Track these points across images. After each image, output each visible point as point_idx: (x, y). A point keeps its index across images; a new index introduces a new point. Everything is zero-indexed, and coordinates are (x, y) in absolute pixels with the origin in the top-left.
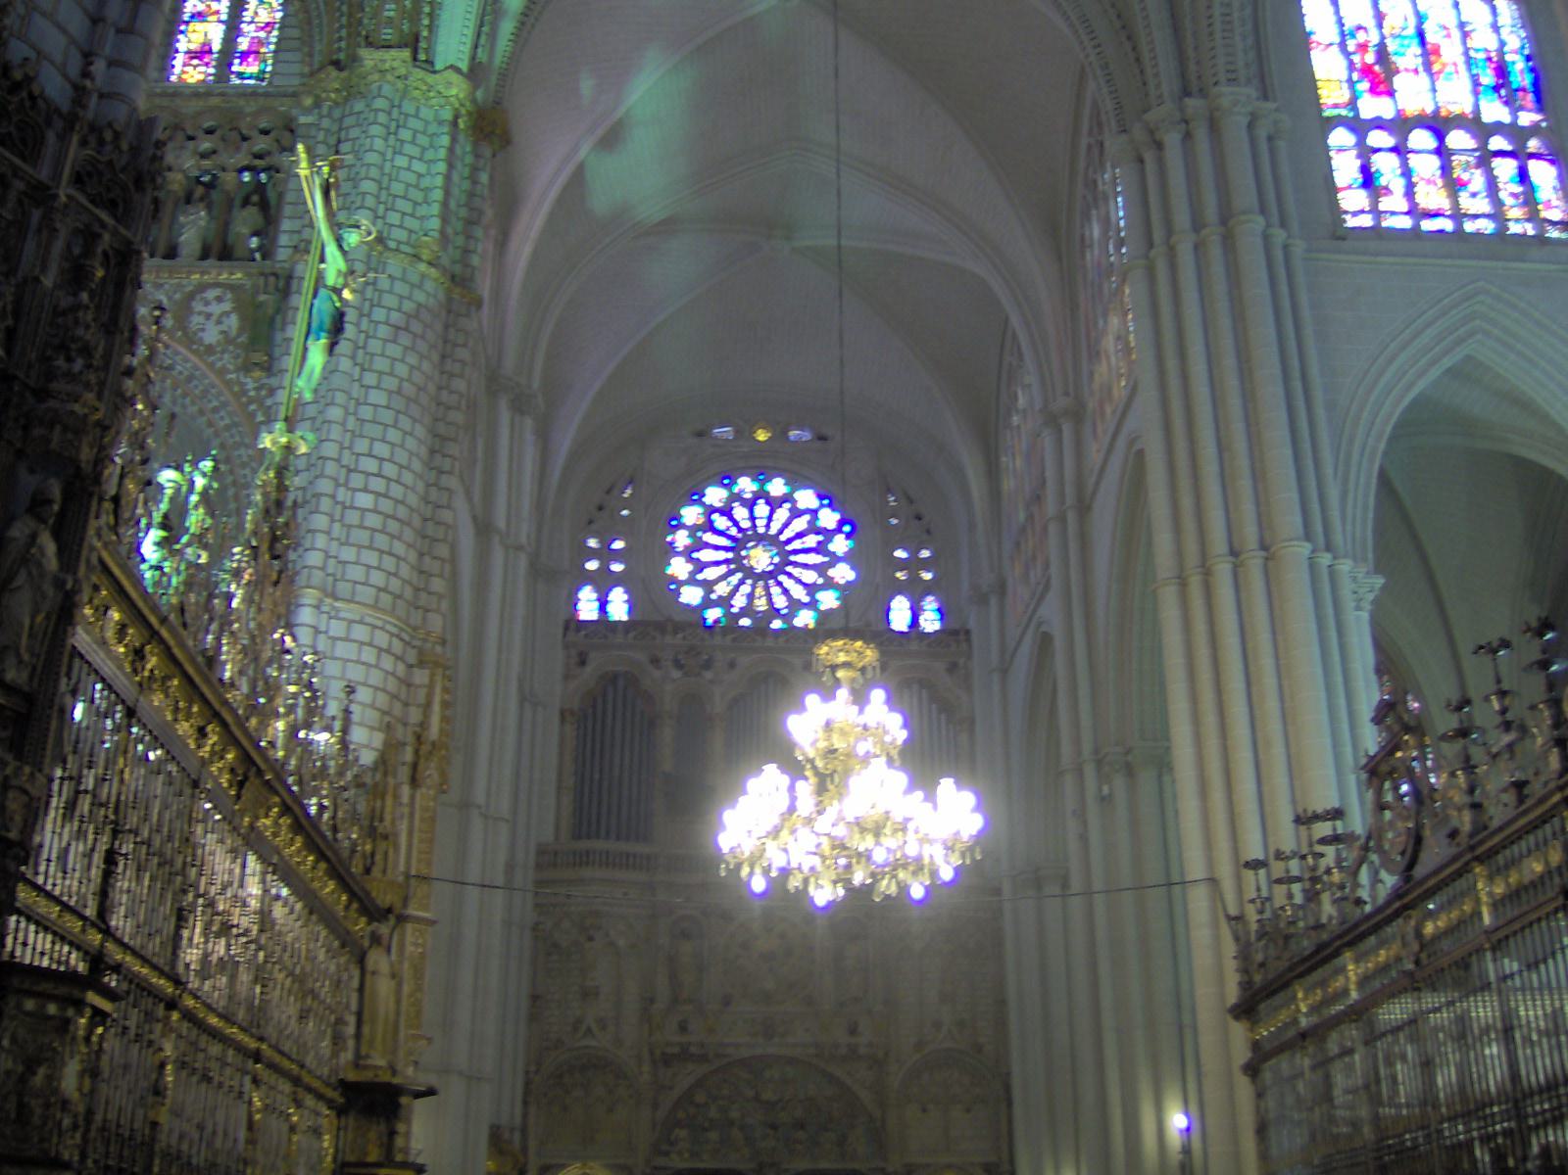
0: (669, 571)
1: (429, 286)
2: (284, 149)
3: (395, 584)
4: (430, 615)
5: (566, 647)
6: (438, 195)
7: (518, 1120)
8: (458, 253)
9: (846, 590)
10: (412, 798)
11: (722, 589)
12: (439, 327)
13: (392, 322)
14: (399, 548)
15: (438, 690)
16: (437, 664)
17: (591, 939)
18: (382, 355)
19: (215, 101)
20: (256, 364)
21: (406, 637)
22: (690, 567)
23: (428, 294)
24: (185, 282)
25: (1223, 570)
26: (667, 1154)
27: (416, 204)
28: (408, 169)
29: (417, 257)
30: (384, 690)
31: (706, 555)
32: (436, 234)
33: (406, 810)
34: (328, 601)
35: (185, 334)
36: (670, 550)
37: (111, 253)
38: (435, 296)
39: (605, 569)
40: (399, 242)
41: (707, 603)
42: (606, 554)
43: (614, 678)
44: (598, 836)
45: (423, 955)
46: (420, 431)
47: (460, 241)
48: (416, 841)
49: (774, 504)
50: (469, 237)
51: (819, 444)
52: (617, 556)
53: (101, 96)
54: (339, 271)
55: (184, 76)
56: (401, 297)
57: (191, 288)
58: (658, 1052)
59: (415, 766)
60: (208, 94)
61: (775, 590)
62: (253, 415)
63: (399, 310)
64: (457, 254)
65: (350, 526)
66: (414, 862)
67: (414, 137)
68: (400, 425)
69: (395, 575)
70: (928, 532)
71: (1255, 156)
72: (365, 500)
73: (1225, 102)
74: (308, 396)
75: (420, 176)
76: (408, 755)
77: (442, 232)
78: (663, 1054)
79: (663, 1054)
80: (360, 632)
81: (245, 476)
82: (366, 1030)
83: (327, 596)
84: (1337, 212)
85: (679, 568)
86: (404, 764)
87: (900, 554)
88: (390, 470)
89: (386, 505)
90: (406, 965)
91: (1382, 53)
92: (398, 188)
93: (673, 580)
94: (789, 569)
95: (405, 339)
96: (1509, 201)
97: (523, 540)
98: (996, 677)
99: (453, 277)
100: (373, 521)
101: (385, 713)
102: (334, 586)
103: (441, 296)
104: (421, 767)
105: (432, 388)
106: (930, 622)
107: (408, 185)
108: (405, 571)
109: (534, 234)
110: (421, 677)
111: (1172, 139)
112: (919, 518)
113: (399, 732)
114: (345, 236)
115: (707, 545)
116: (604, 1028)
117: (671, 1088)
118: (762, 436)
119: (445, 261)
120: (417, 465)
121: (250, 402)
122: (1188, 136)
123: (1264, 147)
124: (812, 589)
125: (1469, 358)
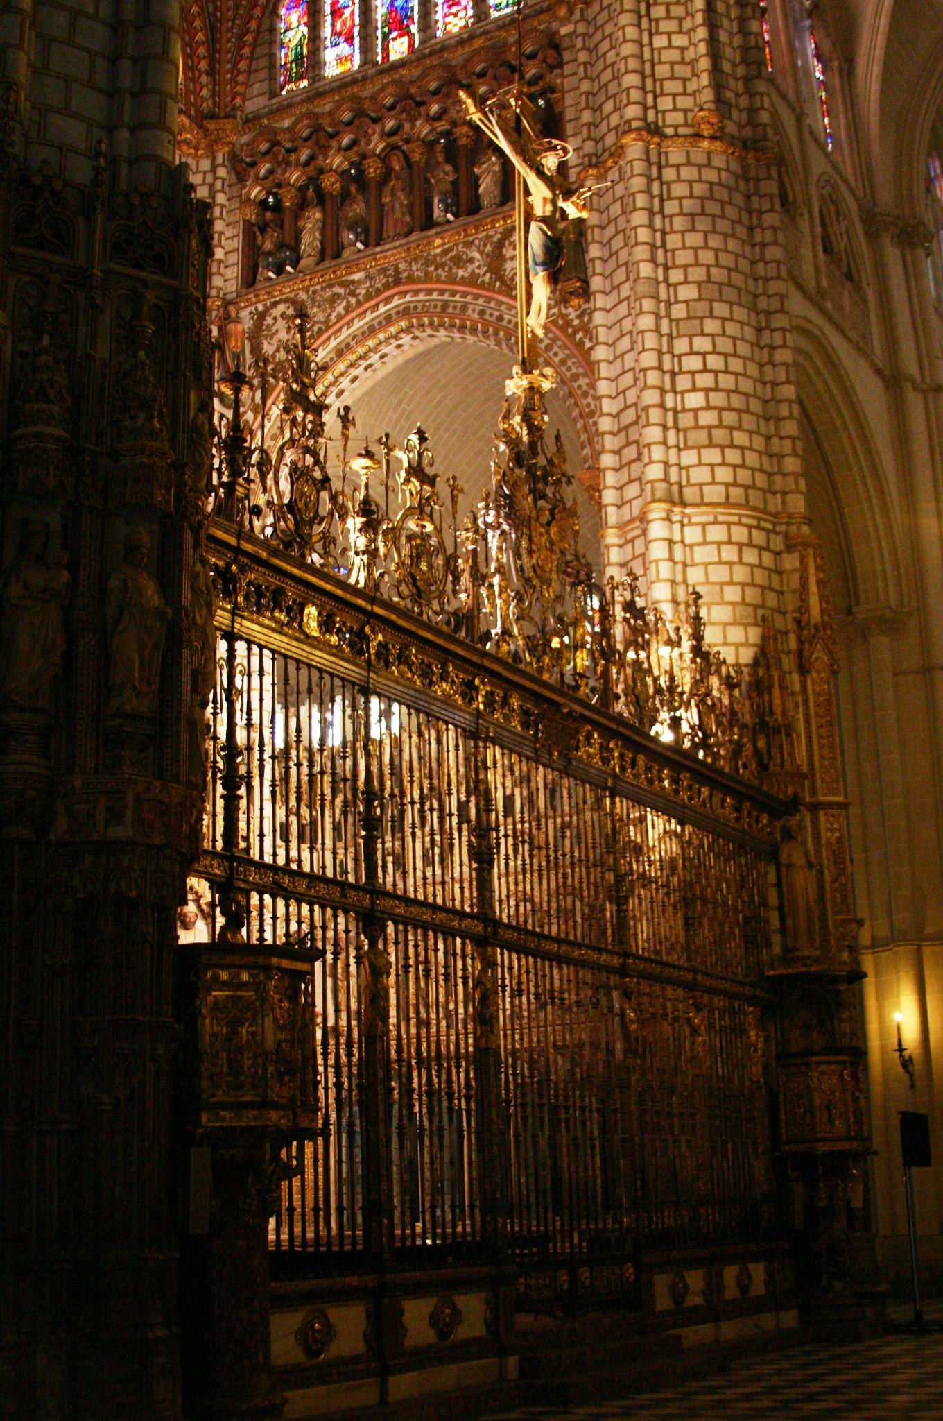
1: (718, 161)
2: (551, 68)
3: (744, 476)
4: (789, 497)
6: (704, 63)
8: (744, 115)
12: (738, 199)
13: (685, 210)
15: (812, 570)
16: (806, 545)
18: (684, 247)
19: (477, 43)
20: (571, 293)
21: (769, 526)
23: (719, 170)
24: (491, 232)
27: (685, 80)
28: (670, 46)
29: (698, 136)
30: (753, 584)
32: (712, 106)
34: (677, 509)
35: (503, 282)
37: (162, 304)
38: (727, 170)
40: (676, 127)
45: (840, 840)
47: (744, 102)
48: (814, 728)
53: (131, 163)
54: (545, 199)
55: (449, 28)
56: (690, 183)
57: (499, 236)
59: (800, 653)
60: (472, 37)
62: (581, 343)
63: (691, 196)
65: (685, 430)
67: (668, 11)
68: (716, 313)
72: (695, 400)
74: (540, 333)
75: (682, 49)
77: (719, 100)
80: (717, 533)
81: (588, 405)
82: (789, 923)
83: (674, 504)
86: (789, 652)
88: (714, 362)
92: (662, 71)
100: (707, 418)
101: (755, 607)
102: (680, 492)
103: (734, 166)
104: (806, 653)
107: (672, 64)
108: (752, 459)
109: (879, 52)
110: (791, 562)
113: (779, 623)
114: (544, 161)
120: (743, 349)
121: (575, 332)
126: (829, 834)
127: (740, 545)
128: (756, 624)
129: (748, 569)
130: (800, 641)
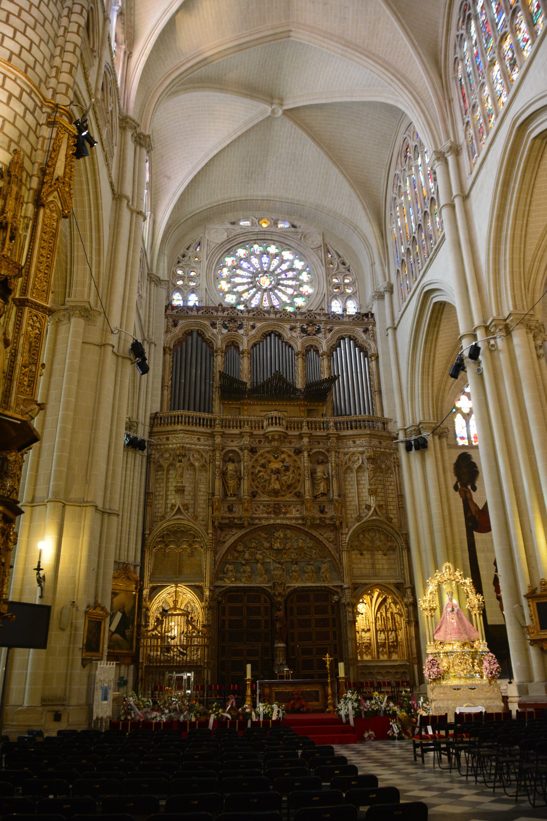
5: (167, 317)
7: (139, 560)
11: (246, 296)
26: (222, 579)
31: (238, 280)
42: (186, 278)
43: (191, 333)
51: (293, 229)
58: (216, 524)
70: (349, 270)
78: (220, 523)
79: (220, 523)
85: (224, 285)
86: (30, 189)
93: (221, 291)
94: (280, 287)
98: (390, 332)
112: (344, 264)
115: (238, 276)
116: (187, 509)
117: (224, 542)
126: (30, 328)
128: (8, 150)
129: (13, 113)
130: (42, 183)
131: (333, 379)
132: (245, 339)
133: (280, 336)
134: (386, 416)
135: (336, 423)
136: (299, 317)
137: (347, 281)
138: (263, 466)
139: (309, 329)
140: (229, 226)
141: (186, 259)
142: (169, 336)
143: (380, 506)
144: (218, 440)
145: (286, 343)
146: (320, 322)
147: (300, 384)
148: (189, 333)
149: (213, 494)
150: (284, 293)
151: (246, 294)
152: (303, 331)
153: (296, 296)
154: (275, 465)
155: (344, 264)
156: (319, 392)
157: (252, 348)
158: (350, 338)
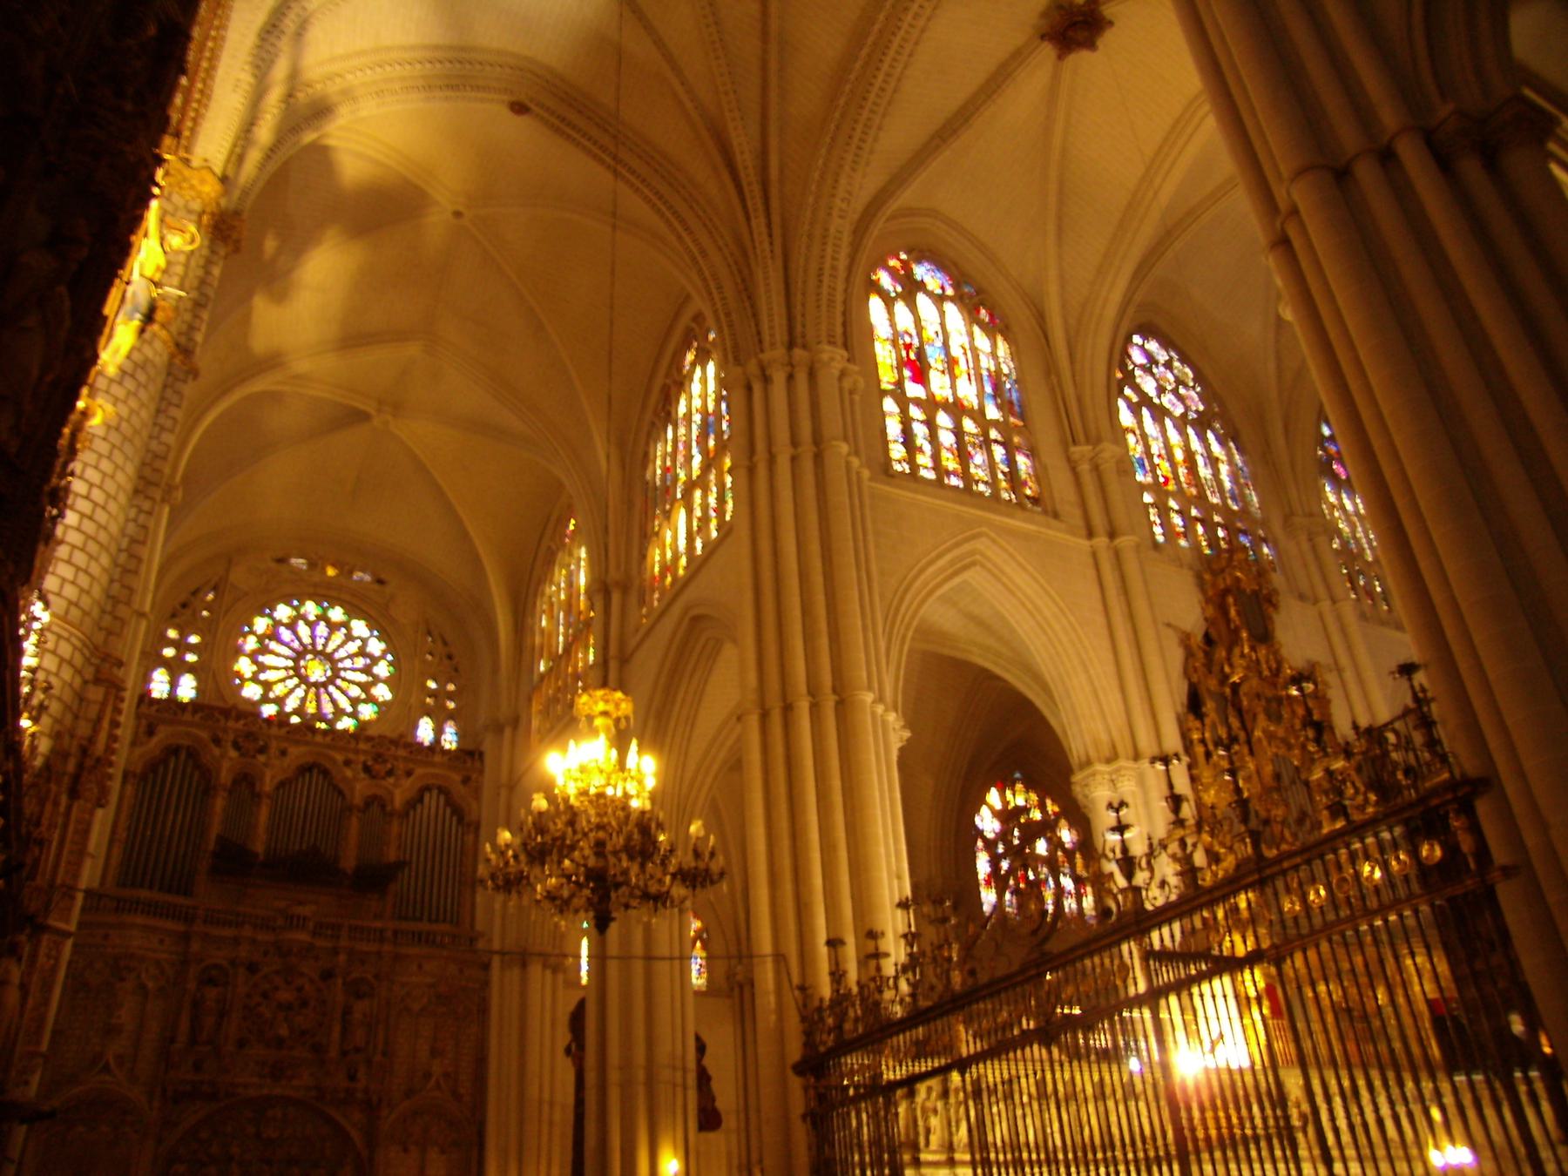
0: (236, 668)
9: (383, 707)
10: (69, 808)
11: (279, 690)
14: (95, 569)
17: (122, 979)
22: (255, 668)
25: (803, 706)
33: (60, 821)
36: (239, 651)
39: (179, 658)
41: (265, 699)
44: (142, 886)
46: (130, 469)
47: (187, 317)
48: (65, 852)
49: (333, 627)
50: (196, 316)
51: (377, 587)
52: (192, 648)
59: (76, 778)
61: (325, 697)
64: (184, 328)
66: (61, 870)
69: (88, 592)
70: (456, 670)
71: (842, 401)
73: (825, 357)
76: (71, 766)
84: (888, 460)
87: (432, 685)
88: (97, 495)
89: (89, 527)
90: (35, 978)
91: (921, 353)
93: (239, 675)
95: (129, 384)
96: (1001, 476)
97: (147, 608)
99: (177, 345)
103: (165, 357)
105: (145, 434)
106: (450, 740)
111: (779, 378)
112: (450, 657)
118: (331, 572)
119: (174, 329)
122: (790, 378)
123: (846, 396)
124: (355, 702)
125: (965, 582)
127: (62, 660)
130: (80, 766)
131: (400, 865)
132: (268, 774)
133: (326, 773)
134: (479, 927)
135: (395, 933)
136: (362, 746)
137: (451, 687)
138: (265, 995)
139: (377, 767)
140: (273, 565)
141: (188, 612)
142: (138, 751)
143: (446, 1075)
144: (195, 946)
145: (335, 787)
146: (396, 758)
147: (349, 862)
148: (174, 750)
149: (172, 1040)
150: (344, 692)
151: (280, 685)
152: (367, 769)
153: (365, 701)
154: (285, 995)
155: (450, 657)
156: (374, 878)
157: (277, 788)
158: (441, 790)
